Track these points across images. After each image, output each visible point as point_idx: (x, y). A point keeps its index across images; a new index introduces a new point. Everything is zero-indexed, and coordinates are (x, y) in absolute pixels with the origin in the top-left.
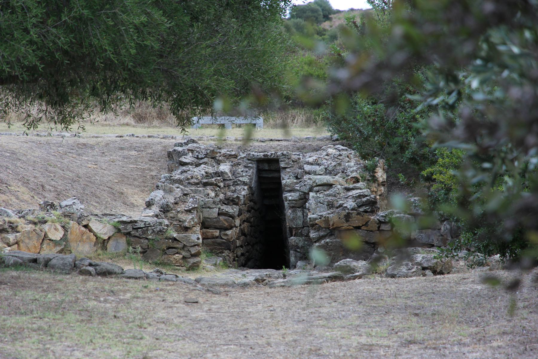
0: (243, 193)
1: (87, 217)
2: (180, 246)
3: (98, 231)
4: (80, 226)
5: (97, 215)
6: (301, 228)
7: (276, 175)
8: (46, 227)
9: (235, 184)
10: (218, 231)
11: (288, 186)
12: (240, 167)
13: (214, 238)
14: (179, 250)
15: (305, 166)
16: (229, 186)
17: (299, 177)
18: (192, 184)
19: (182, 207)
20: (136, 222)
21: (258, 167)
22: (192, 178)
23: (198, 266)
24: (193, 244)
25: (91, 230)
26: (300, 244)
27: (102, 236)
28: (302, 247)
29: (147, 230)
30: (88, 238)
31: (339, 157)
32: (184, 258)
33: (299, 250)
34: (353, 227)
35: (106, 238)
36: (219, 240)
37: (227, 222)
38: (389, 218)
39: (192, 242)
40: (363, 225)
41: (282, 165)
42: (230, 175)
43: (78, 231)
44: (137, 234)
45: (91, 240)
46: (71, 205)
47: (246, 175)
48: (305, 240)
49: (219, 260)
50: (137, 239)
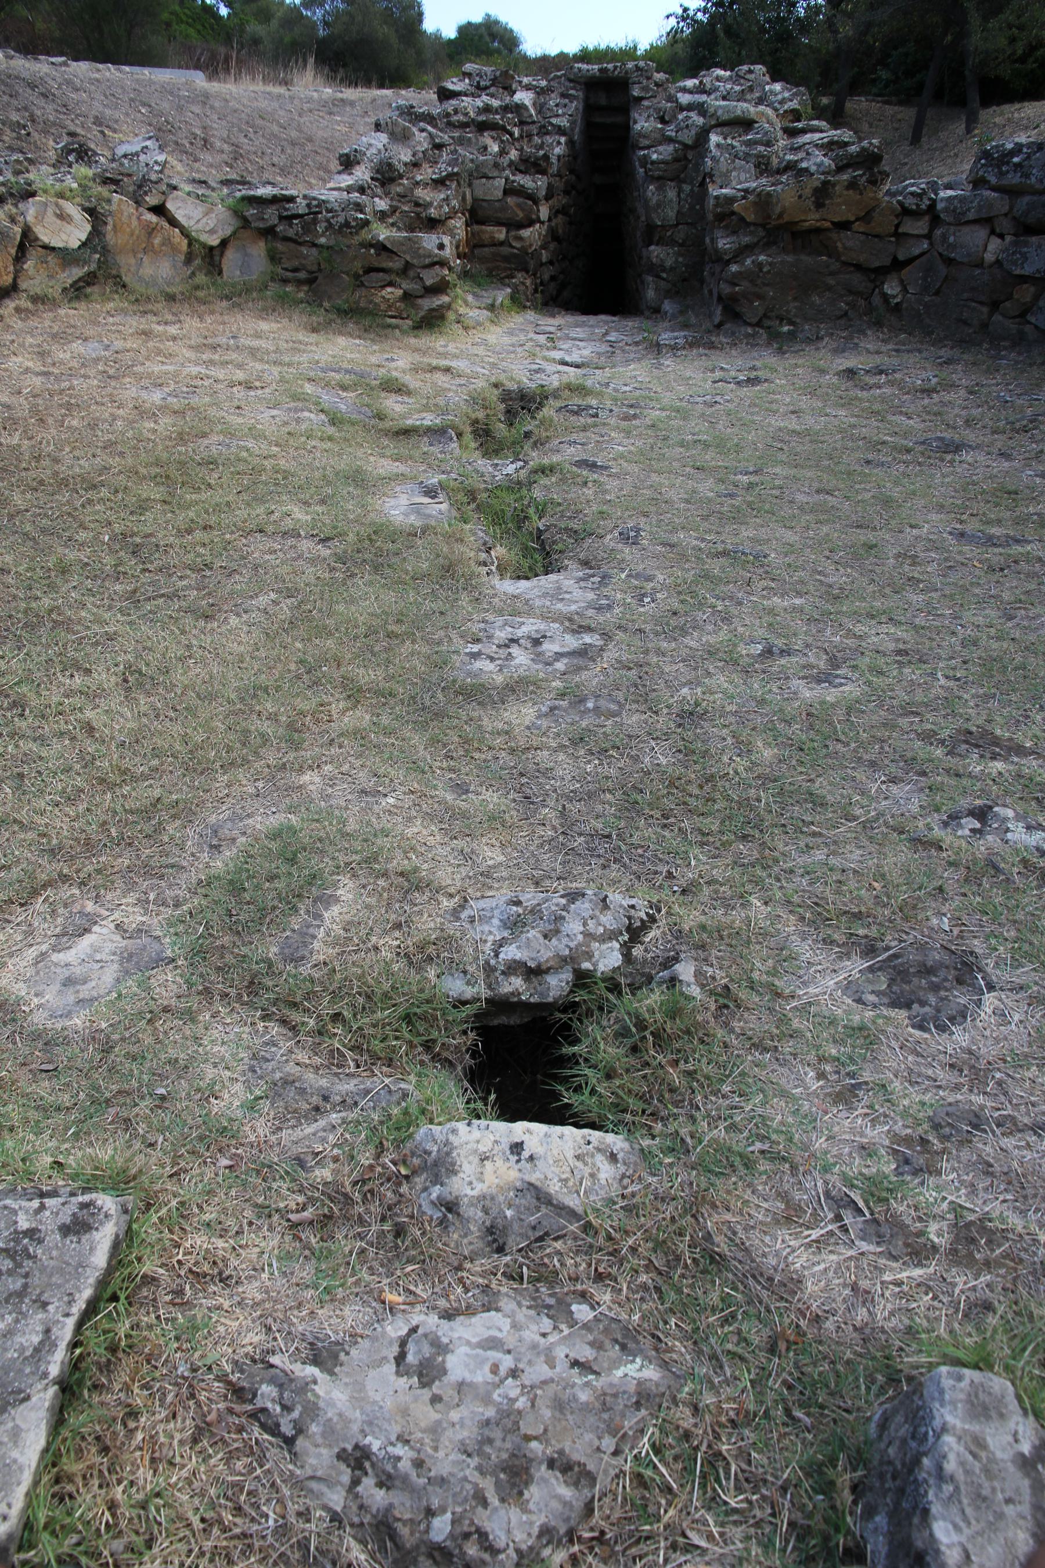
0: (558, 150)
1: (156, 183)
2: (396, 264)
3: (192, 223)
4: (141, 209)
5: (204, 182)
6: (671, 226)
7: (619, 119)
8: (30, 210)
9: (543, 131)
10: (504, 230)
11: (644, 137)
12: (553, 95)
13: (495, 245)
14: (393, 277)
15: (679, 95)
16: (530, 136)
17: (667, 118)
18: (455, 127)
19: (427, 173)
20: (291, 199)
21: (586, 99)
22: (456, 112)
23: (442, 317)
24: (427, 261)
25: (173, 222)
26: (669, 263)
27: (204, 238)
28: (672, 269)
29: (315, 221)
30: (167, 241)
31: (748, 76)
32: (407, 296)
33: (664, 275)
34: (833, 223)
35: (214, 241)
36: (505, 250)
37: (523, 210)
38: (930, 199)
39: (425, 256)
40: (857, 220)
41: (636, 92)
42: (533, 112)
43: (135, 223)
44: (291, 233)
45: (175, 249)
46: (137, 154)
47: (564, 114)
48: (679, 254)
49: (502, 295)
50: (292, 245)
